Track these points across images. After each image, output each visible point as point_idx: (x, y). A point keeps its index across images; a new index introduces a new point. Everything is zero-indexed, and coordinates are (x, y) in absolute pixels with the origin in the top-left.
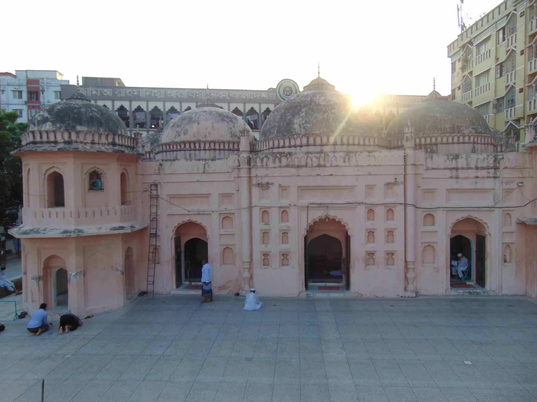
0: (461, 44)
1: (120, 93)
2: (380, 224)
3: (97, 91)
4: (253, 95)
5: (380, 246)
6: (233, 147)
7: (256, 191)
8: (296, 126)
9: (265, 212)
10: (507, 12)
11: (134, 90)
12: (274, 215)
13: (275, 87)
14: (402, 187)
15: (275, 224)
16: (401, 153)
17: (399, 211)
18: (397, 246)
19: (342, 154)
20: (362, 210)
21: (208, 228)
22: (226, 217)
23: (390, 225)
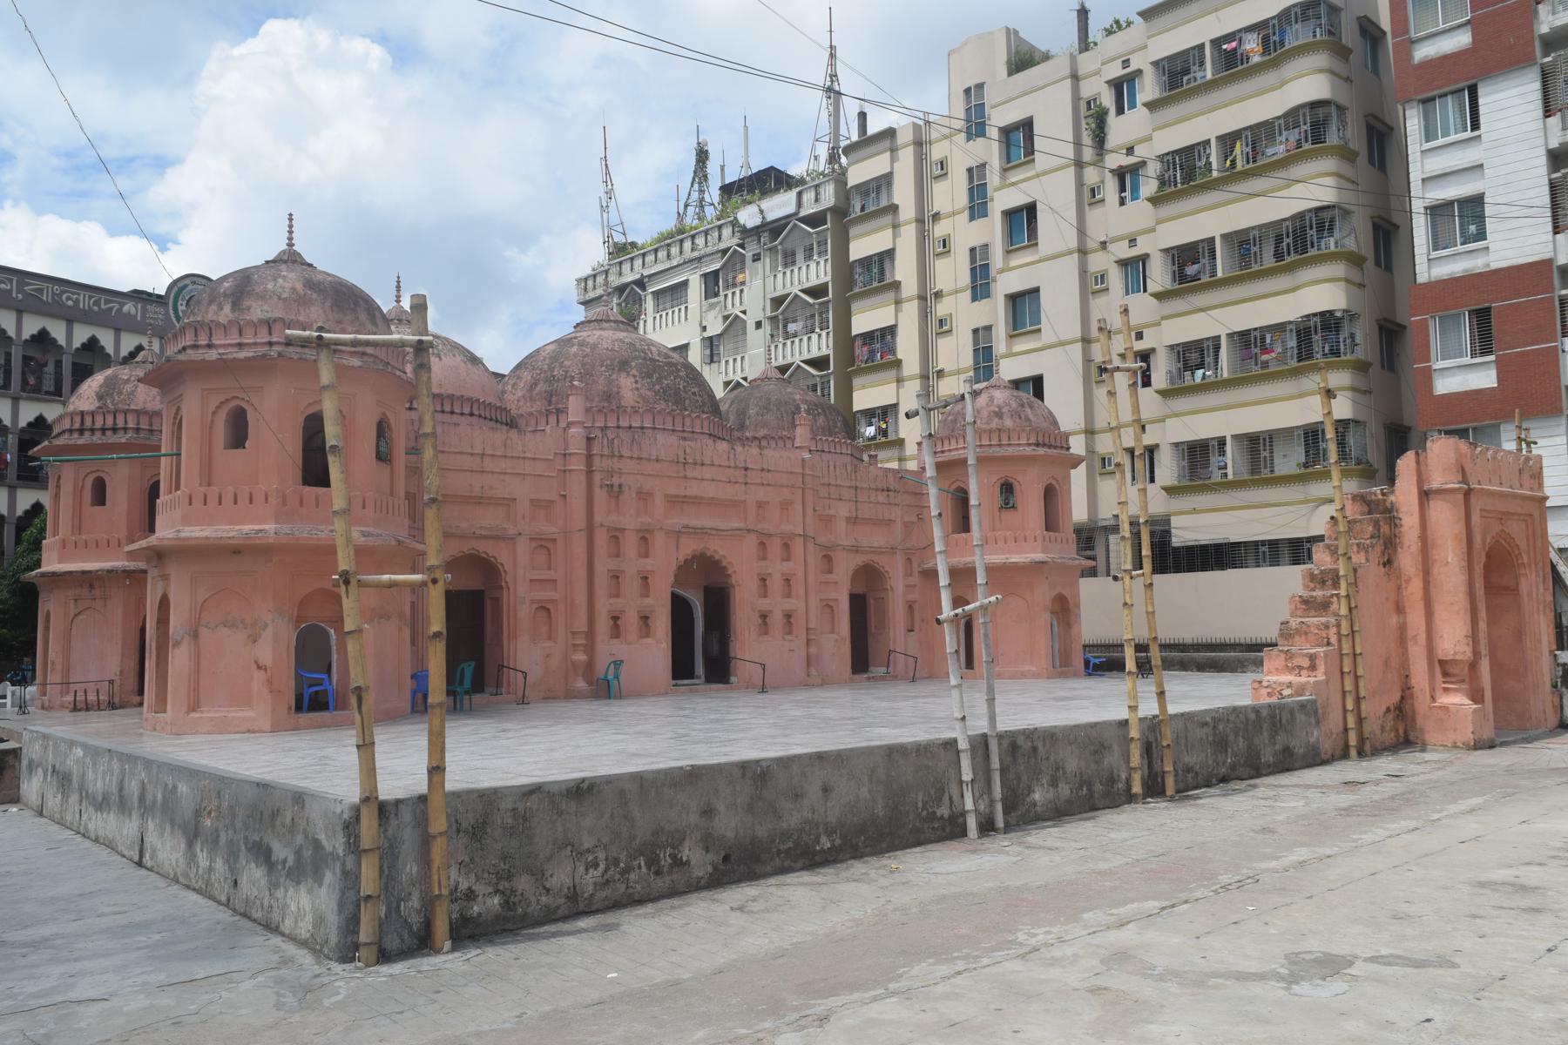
0: (615, 281)
2: (777, 568)
4: (97, 303)
5: (777, 604)
7: (600, 496)
9: (615, 537)
10: (723, 246)
12: (630, 544)
13: (162, 292)
14: (799, 508)
15: (632, 563)
17: (798, 546)
18: (796, 603)
20: (751, 541)
23: (787, 567)
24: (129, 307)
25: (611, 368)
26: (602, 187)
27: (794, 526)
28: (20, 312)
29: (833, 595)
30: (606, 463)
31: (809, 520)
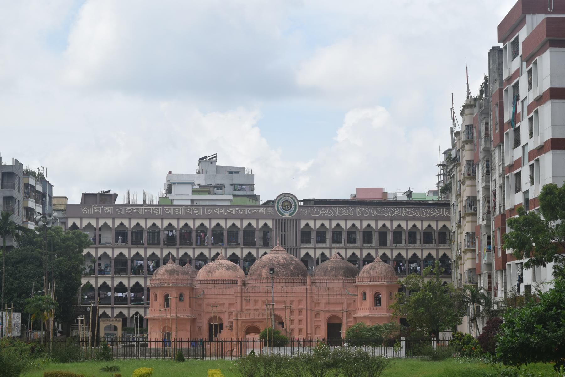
1: (120, 210)
2: (296, 317)
3: (99, 209)
4: (250, 211)
6: (233, 282)
7: (244, 302)
8: (263, 274)
11: (134, 208)
14: (305, 301)
16: (305, 287)
17: (304, 312)
18: (303, 326)
19: (280, 287)
20: (288, 311)
21: (223, 319)
22: (231, 314)
23: (300, 317)
24: (261, 210)
25: (262, 268)
26: (451, 122)
27: (303, 306)
28: (226, 219)
29: (320, 324)
30: (245, 295)
31: (308, 305)
